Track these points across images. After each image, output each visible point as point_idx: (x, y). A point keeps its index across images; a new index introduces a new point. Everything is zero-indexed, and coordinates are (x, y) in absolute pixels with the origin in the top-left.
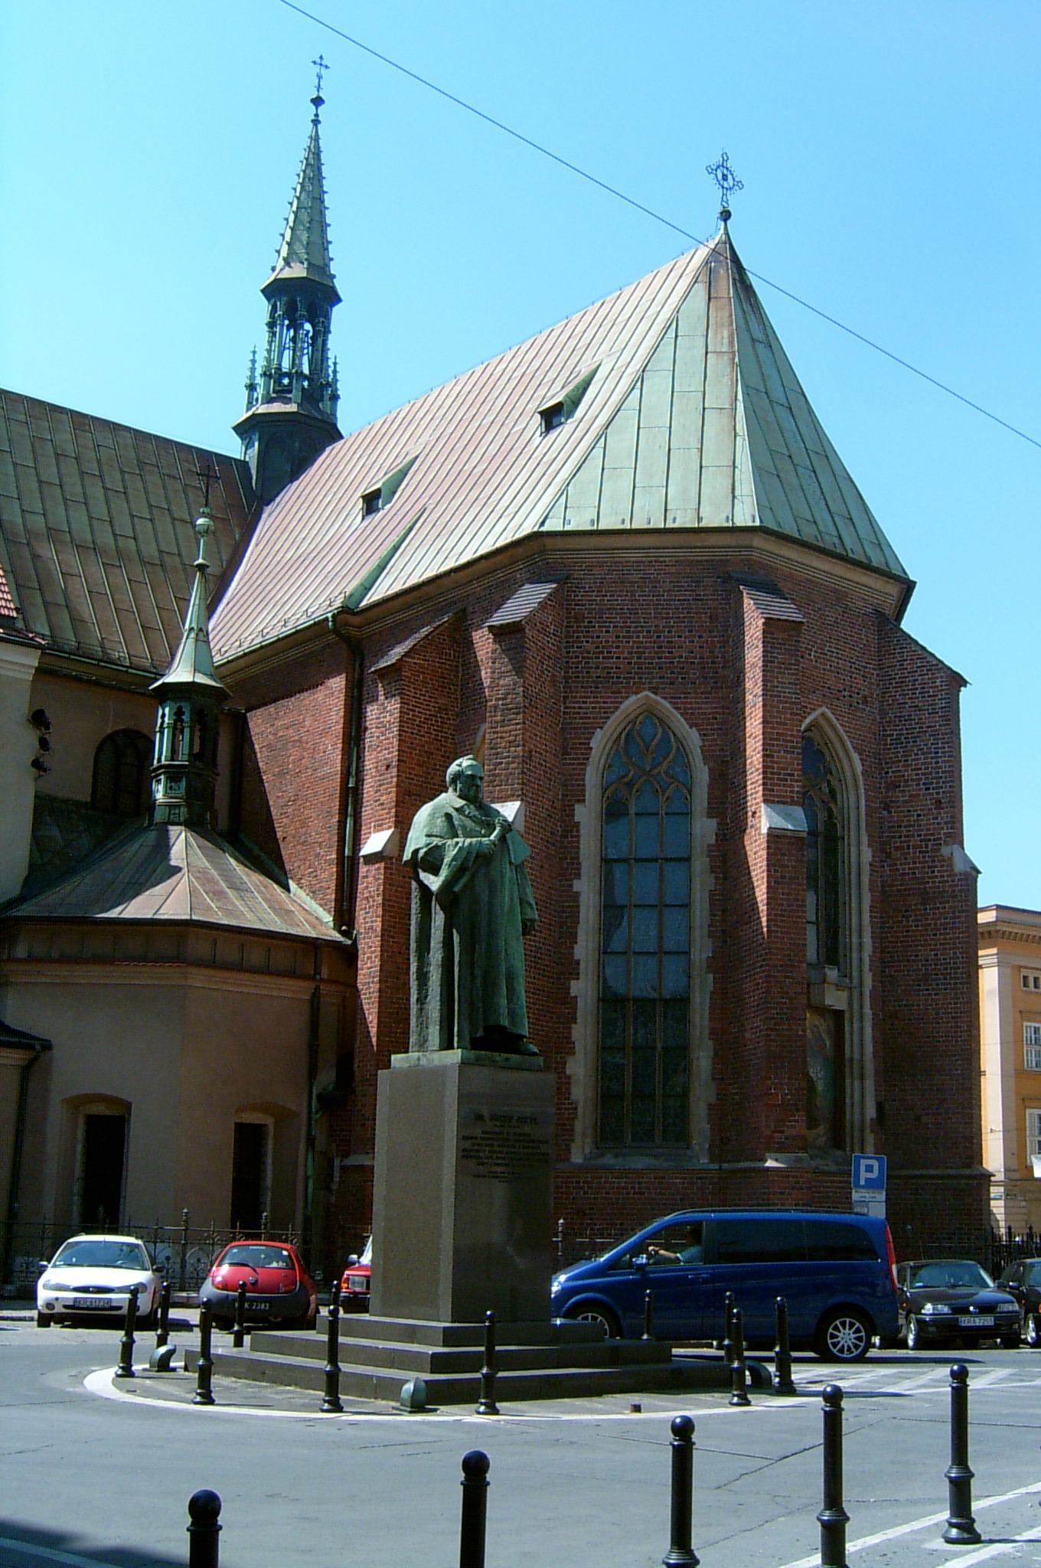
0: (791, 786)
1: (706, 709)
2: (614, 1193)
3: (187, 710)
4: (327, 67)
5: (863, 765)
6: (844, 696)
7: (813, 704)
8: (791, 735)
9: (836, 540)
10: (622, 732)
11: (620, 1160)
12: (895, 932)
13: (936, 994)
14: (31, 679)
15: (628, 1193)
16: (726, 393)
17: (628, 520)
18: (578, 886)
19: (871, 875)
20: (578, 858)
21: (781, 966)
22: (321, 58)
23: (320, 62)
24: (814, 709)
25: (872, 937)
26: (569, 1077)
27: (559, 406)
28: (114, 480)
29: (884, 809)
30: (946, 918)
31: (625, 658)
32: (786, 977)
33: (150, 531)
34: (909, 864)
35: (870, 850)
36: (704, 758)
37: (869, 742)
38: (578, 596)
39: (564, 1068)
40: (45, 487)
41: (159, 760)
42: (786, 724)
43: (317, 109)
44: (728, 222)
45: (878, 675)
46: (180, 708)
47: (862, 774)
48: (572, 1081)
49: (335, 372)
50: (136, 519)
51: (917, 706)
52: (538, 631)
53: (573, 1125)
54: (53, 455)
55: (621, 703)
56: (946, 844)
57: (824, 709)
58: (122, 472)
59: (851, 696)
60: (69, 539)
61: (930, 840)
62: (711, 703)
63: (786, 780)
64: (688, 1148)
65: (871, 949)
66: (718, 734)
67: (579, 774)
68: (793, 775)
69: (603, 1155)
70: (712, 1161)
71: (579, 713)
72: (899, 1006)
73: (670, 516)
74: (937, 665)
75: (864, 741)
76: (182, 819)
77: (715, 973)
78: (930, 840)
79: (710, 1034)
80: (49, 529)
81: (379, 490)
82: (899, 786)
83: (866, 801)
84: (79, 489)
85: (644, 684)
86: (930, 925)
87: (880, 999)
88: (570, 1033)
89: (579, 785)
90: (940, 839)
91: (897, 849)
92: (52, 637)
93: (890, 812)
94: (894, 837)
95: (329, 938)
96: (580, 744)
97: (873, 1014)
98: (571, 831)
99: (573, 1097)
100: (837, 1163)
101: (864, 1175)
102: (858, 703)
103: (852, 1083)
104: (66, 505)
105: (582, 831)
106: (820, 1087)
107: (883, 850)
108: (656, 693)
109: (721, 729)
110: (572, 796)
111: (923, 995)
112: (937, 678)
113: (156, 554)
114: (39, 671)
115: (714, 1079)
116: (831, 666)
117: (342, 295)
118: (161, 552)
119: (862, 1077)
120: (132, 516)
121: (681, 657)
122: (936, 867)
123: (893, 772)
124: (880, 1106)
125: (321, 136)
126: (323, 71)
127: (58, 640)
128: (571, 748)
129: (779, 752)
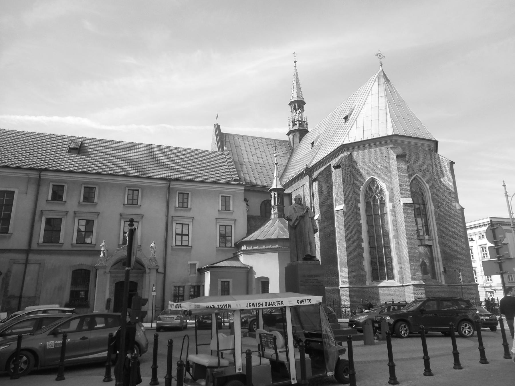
0: (407, 193)
4: (296, 54)
9: (415, 134)
10: (367, 186)
16: (384, 105)
17: (362, 139)
18: (361, 222)
19: (435, 212)
20: (360, 216)
21: (410, 236)
22: (295, 52)
23: (295, 54)
24: (414, 175)
25: (437, 227)
27: (347, 116)
29: (436, 196)
30: (456, 221)
31: (366, 169)
34: (444, 208)
35: (434, 206)
36: (387, 189)
39: (362, 264)
40: (248, 153)
44: (382, 66)
46: (275, 194)
47: (429, 188)
48: (365, 267)
49: (306, 119)
57: (417, 174)
59: (424, 170)
61: (449, 202)
62: (388, 177)
63: (406, 192)
66: (390, 184)
68: (408, 191)
70: (400, 283)
71: (357, 183)
72: (446, 243)
73: (372, 136)
74: (446, 160)
76: (277, 217)
77: (395, 238)
78: (449, 202)
81: (314, 142)
83: (431, 194)
86: (452, 223)
87: (440, 242)
88: (363, 255)
89: (359, 199)
91: (441, 205)
93: (438, 197)
94: (440, 202)
99: (365, 270)
100: (434, 283)
103: (436, 263)
105: (360, 210)
106: (428, 264)
107: (437, 207)
109: (390, 182)
110: (358, 202)
111: (453, 240)
112: (446, 163)
114: (245, 190)
115: (398, 264)
117: (306, 102)
119: (439, 261)
121: (379, 167)
122: (452, 208)
123: (438, 187)
124: (445, 268)
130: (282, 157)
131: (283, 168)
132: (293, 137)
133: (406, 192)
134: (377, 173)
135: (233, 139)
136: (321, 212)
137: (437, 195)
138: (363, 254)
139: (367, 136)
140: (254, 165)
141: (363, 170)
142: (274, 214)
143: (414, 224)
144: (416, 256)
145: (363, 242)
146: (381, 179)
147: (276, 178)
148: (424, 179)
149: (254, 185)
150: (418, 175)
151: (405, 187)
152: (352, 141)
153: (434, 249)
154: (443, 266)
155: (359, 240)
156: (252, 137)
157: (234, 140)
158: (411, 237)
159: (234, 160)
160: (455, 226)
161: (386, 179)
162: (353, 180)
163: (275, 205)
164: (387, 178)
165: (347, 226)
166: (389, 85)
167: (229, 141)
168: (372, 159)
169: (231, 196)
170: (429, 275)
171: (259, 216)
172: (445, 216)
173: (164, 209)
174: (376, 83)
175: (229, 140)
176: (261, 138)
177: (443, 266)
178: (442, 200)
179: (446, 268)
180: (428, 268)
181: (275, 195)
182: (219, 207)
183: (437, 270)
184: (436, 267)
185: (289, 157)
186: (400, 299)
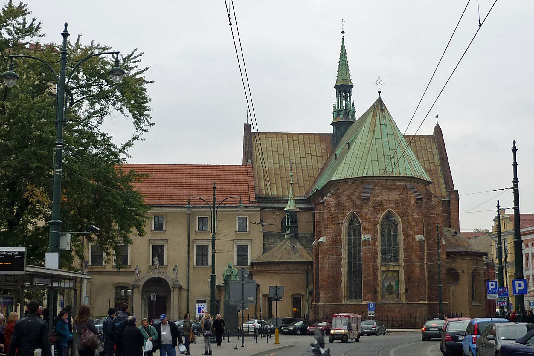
3: (289, 215)
4: (344, 22)
23: (343, 21)
28: (297, 149)
41: (288, 224)
60: (284, 168)
106: (394, 286)
113: (306, 166)
124: (406, 289)
125: (344, 42)
130: (320, 157)
131: (318, 173)
135: (265, 139)
149: (280, 197)
150: (391, 209)
157: (266, 140)
166: (382, 116)
170: (395, 294)
173: (186, 234)
174: (372, 113)
176: (298, 134)
181: (288, 215)
182: (236, 229)
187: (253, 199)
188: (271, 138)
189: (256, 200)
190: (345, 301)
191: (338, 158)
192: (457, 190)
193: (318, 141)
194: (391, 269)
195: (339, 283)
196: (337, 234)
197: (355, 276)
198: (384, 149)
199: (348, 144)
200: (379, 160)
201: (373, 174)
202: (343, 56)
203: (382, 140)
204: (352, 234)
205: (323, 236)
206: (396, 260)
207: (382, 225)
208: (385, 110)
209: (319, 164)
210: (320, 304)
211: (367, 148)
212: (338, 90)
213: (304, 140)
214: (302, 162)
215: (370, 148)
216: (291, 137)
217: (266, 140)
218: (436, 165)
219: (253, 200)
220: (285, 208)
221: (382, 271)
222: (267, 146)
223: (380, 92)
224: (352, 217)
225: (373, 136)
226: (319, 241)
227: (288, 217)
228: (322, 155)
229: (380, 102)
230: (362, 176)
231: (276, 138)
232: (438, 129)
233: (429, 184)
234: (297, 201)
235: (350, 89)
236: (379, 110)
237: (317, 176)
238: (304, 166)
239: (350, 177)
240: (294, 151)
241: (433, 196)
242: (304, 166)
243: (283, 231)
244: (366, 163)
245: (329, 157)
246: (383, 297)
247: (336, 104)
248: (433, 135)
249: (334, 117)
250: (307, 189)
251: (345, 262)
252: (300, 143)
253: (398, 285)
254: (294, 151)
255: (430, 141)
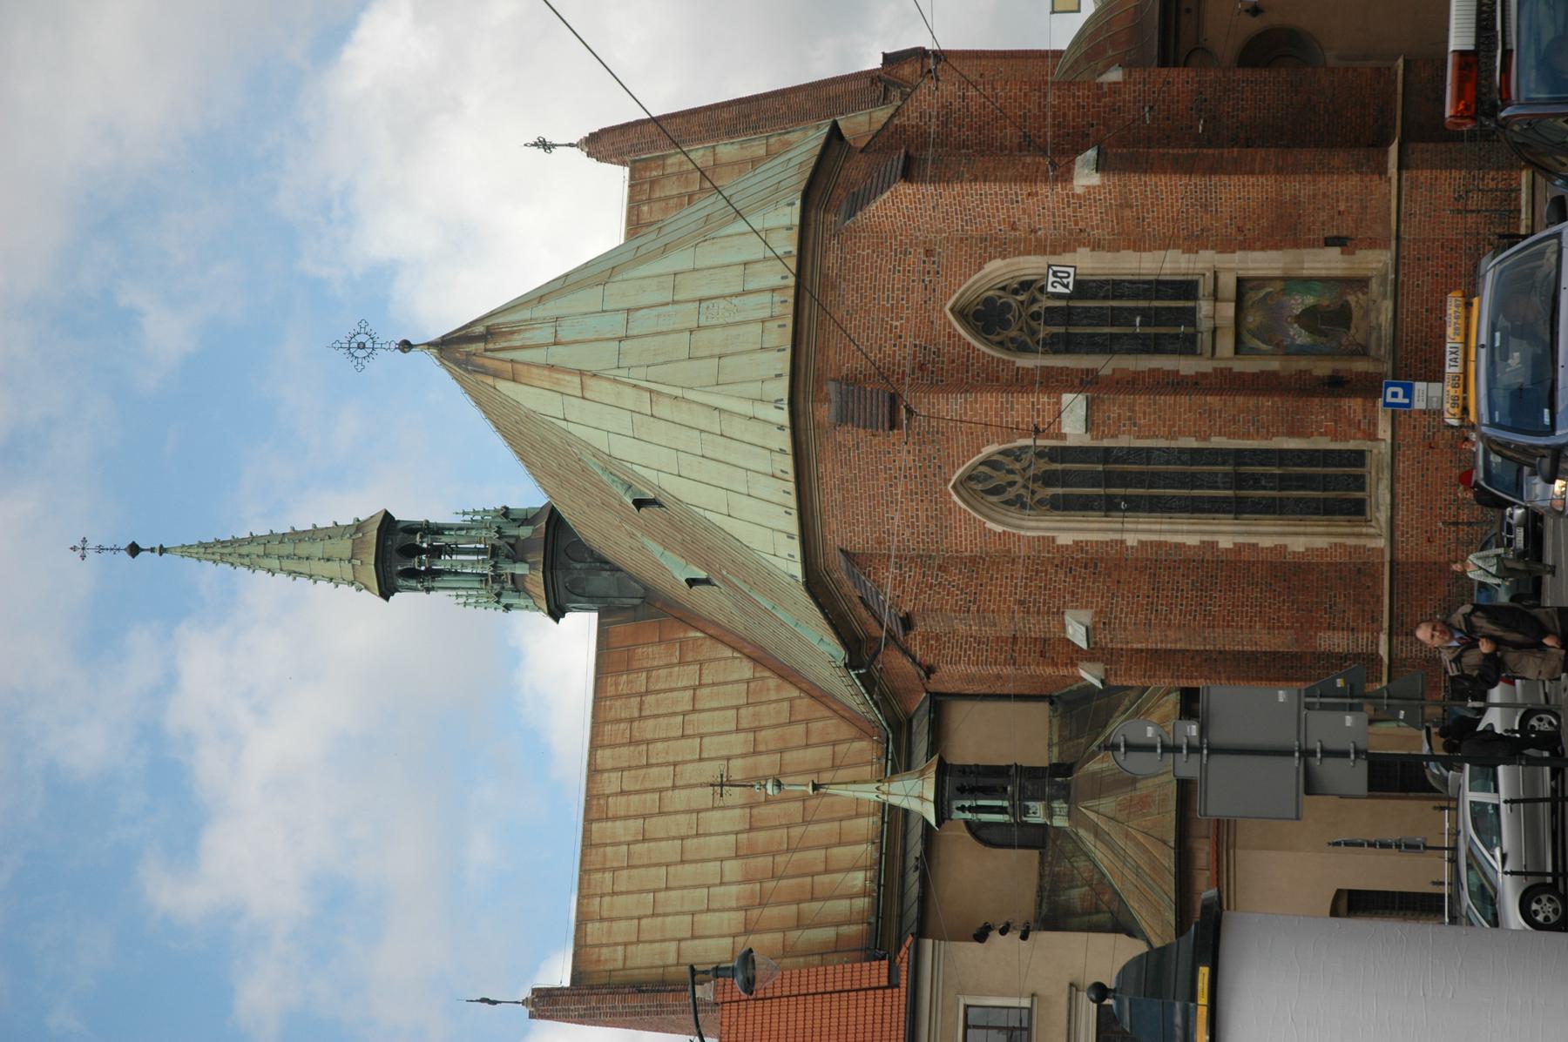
1: (963, 439)
2: (1413, 514)
3: (960, 803)
4: (84, 541)
5: (995, 257)
6: (930, 281)
7: (945, 323)
8: (997, 404)
9: (777, 297)
11: (1382, 508)
12: (1159, 226)
13: (1221, 199)
14: (942, 942)
15: (1412, 503)
19: (1103, 249)
20: (1107, 542)
22: (74, 549)
23: (82, 549)
26: (1307, 550)
29: (1036, 232)
31: (917, 504)
32: (1220, 417)
33: (716, 739)
37: (971, 248)
38: (859, 543)
39: (1299, 553)
41: (1002, 810)
42: (986, 408)
43: (143, 550)
44: (412, 343)
45: (901, 235)
46: (958, 809)
47: (1004, 257)
48: (1310, 546)
50: (705, 755)
51: (934, 207)
52: (903, 593)
53: (1350, 546)
54: (646, 845)
55: (960, 508)
56: (1073, 189)
58: (648, 765)
60: (745, 836)
61: (1068, 202)
62: (957, 436)
64: (1371, 451)
65: (1176, 251)
67: (1029, 541)
68: (1033, 403)
69: (1377, 519)
71: (971, 541)
73: (779, 474)
74: (892, 192)
75: (971, 255)
76: (1065, 805)
78: (1068, 202)
79: (1266, 439)
80: (737, 856)
82: (1014, 222)
84: (681, 818)
85: (941, 490)
88: (1267, 548)
89: (1039, 541)
90: (1067, 194)
91: (1076, 223)
92: (866, 870)
93: (1040, 229)
94: (1065, 227)
95: (1179, 707)
96: (1000, 539)
97: (1240, 249)
98: (1082, 547)
99: (1325, 546)
101: (1400, 400)
102: (934, 263)
104: (705, 835)
106: (1310, 300)
108: (950, 480)
113: (742, 736)
116: (903, 299)
118: (738, 730)
120: (701, 759)
122: (1095, 198)
124: (1330, 242)
126: (91, 544)
127: (868, 863)
128: (1005, 546)
129: (1012, 416)
130: (705, 672)
131: (773, 682)
132: (580, 598)
133: (1038, 410)
134: (940, 467)
135: (606, 924)
136: (1072, 659)
137: (1034, 231)
138: (1262, 548)
139: (784, 492)
140: (761, 836)
141: (917, 515)
142: (1050, 813)
143: (1165, 402)
144: (1287, 410)
145: (1213, 545)
146: (964, 456)
147: (884, 797)
148: (965, 281)
149: (878, 855)
150: (949, 304)
151: (1018, 410)
152: (795, 547)
153: (1254, 269)
154: (1319, 247)
155: (1204, 553)
156: (588, 820)
157: (611, 919)
158: (1215, 421)
159: (733, 931)
160: (1167, 197)
161: (968, 441)
162: (957, 551)
163: (1010, 810)
164: (963, 439)
165: (1152, 613)
166: (516, 336)
167: (620, 948)
168: (877, 480)
169: (964, 1000)
170: (1351, 299)
171: (1042, 856)
172: (1122, 217)
174: (505, 387)
175: (616, 944)
177: (1322, 248)
178: (1054, 217)
179: (1327, 234)
180: (1326, 303)
181: (962, 809)
183: (1336, 269)
184: (1323, 273)
185: (699, 634)
186: (1441, 446)
187: (877, 972)
188: (602, 896)
189: (883, 958)
190: (1372, 531)
191: (707, 566)
192: (881, 56)
193: (629, 682)
194: (1228, 310)
195: (1289, 558)
196: (1056, 562)
197: (1256, 481)
198: (670, 328)
199: (640, 503)
200: (717, 351)
201: (780, 375)
202: (244, 550)
203: (627, 337)
204: (1060, 491)
205: (1064, 626)
206: (1186, 288)
207: (1023, 348)
208: (489, 323)
209: (735, 677)
210: (1383, 651)
211: (664, 409)
212: (400, 582)
213: (620, 745)
214: (720, 754)
215: (659, 393)
216: (602, 802)
217: (611, 919)
218: (762, 152)
219: (885, 971)
220: (926, 823)
221: (1237, 352)
222: (641, 912)
223: (406, 346)
224: (979, 487)
225: (609, 379)
226: (1084, 645)
227: (971, 809)
228: (694, 662)
229: (451, 347)
230: (788, 431)
231: (603, 870)
232: (601, 144)
233: (841, 138)
234: (898, 762)
235: (400, 526)
236: (486, 350)
237: (787, 686)
238: (738, 743)
239: (791, 487)
240: (667, 789)
241: (896, 121)
242: (738, 743)
243: (1037, 838)
244: (731, 413)
245: (702, 631)
246: (1362, 352)
247: (464, 593)
248: (627, 169)
249: (522, 602)
250: (846, 731)
251: (1185, 527)
252: (634, 764)
253: (1306, 282)
254: (667, 789)
255: (653, 183)
